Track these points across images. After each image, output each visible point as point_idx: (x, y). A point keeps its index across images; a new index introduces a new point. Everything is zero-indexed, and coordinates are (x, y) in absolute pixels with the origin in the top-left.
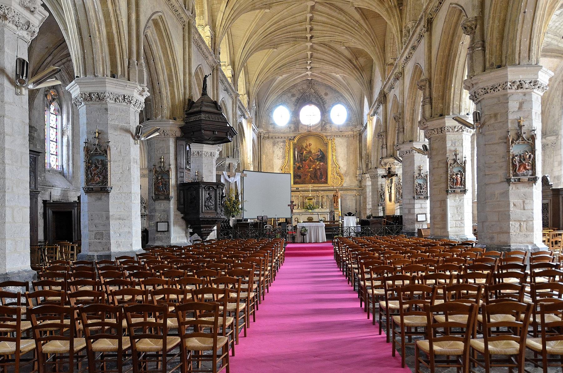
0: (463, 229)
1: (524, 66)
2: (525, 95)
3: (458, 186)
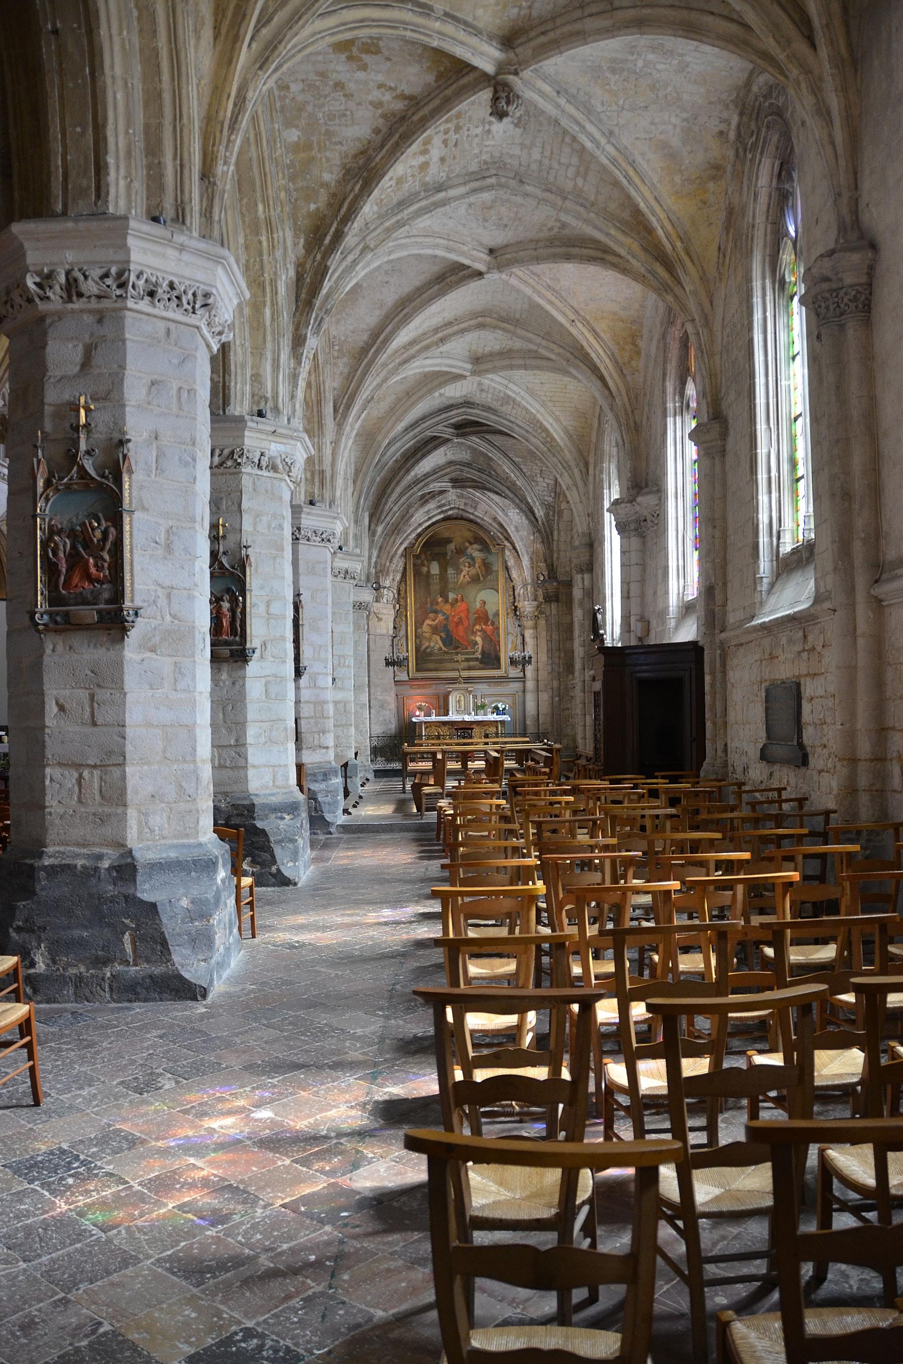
0: (242, 772)
1: (78, 218)
2: (100, 321)
3: (225, 637)
